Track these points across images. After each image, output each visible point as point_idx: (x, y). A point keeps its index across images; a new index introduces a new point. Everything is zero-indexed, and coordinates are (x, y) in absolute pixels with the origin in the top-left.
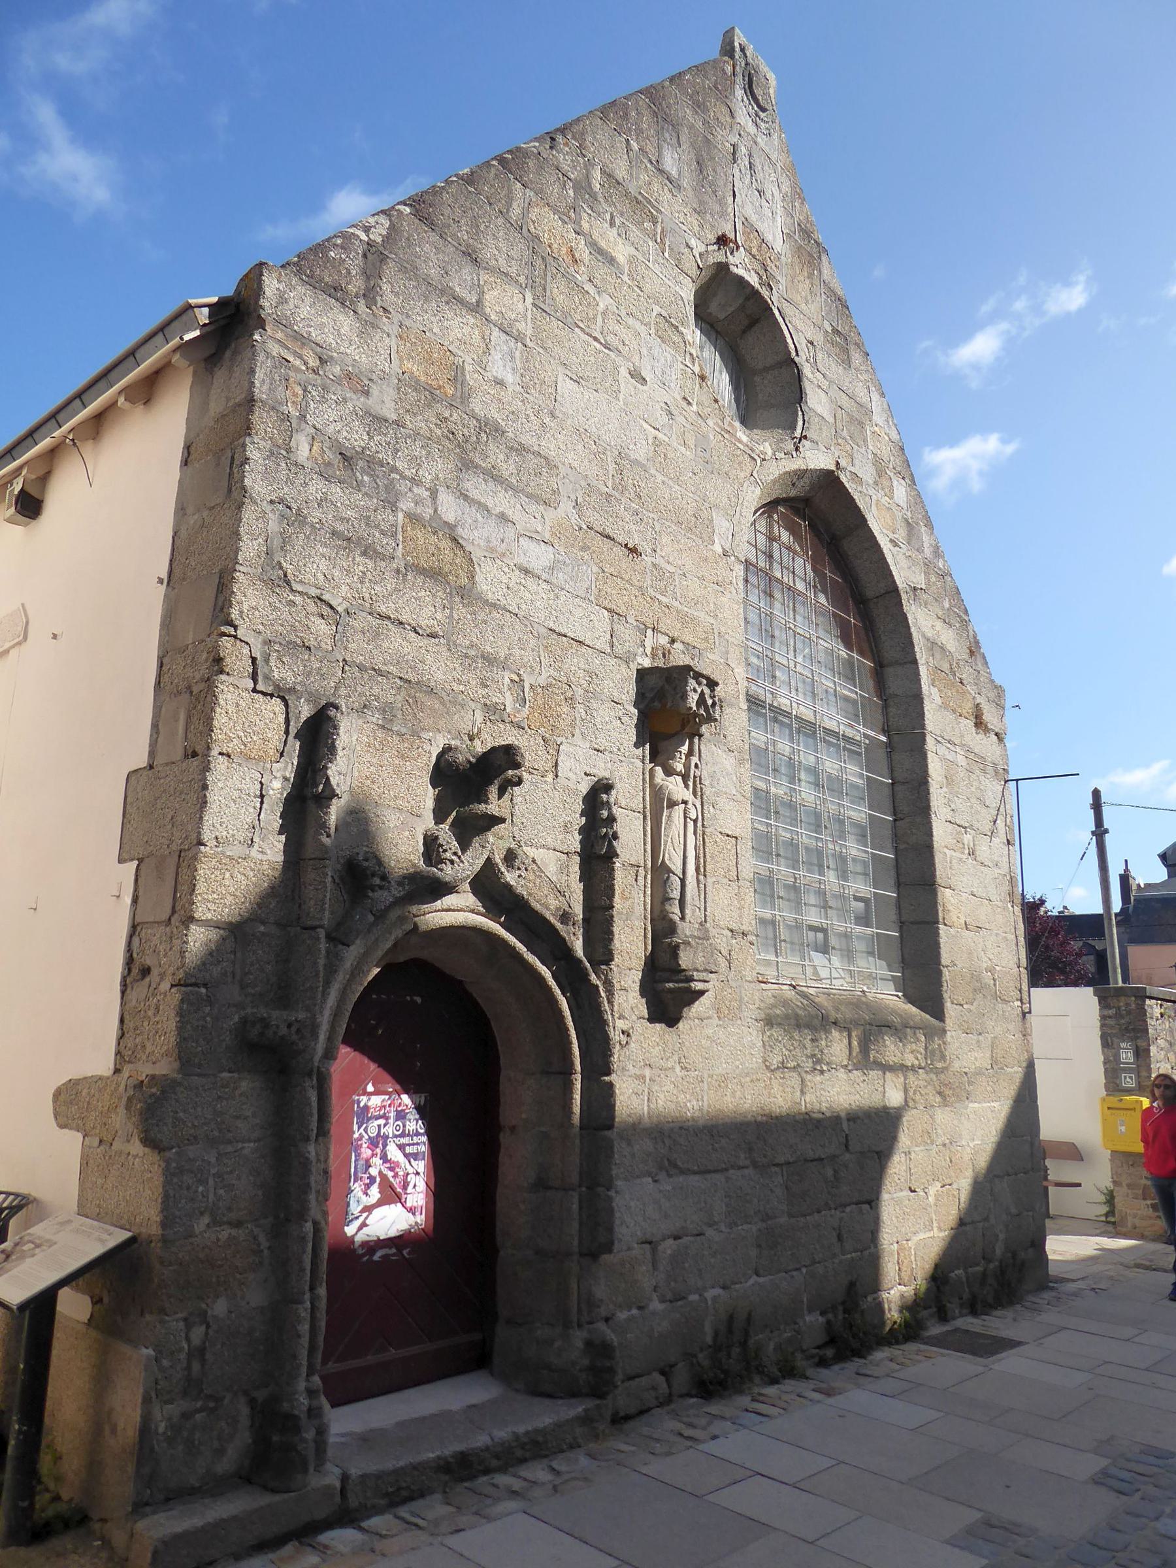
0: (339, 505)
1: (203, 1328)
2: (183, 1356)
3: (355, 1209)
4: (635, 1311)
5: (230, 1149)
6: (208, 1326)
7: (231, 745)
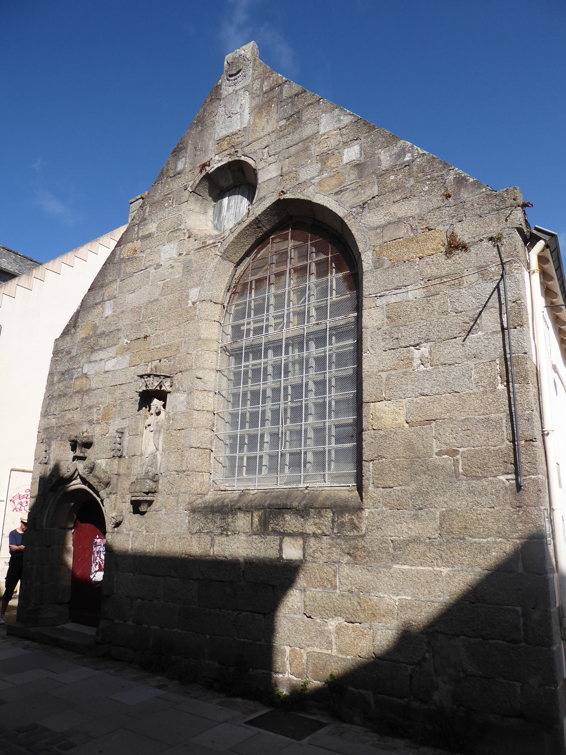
3: (93, 571)
4: (122, 622)
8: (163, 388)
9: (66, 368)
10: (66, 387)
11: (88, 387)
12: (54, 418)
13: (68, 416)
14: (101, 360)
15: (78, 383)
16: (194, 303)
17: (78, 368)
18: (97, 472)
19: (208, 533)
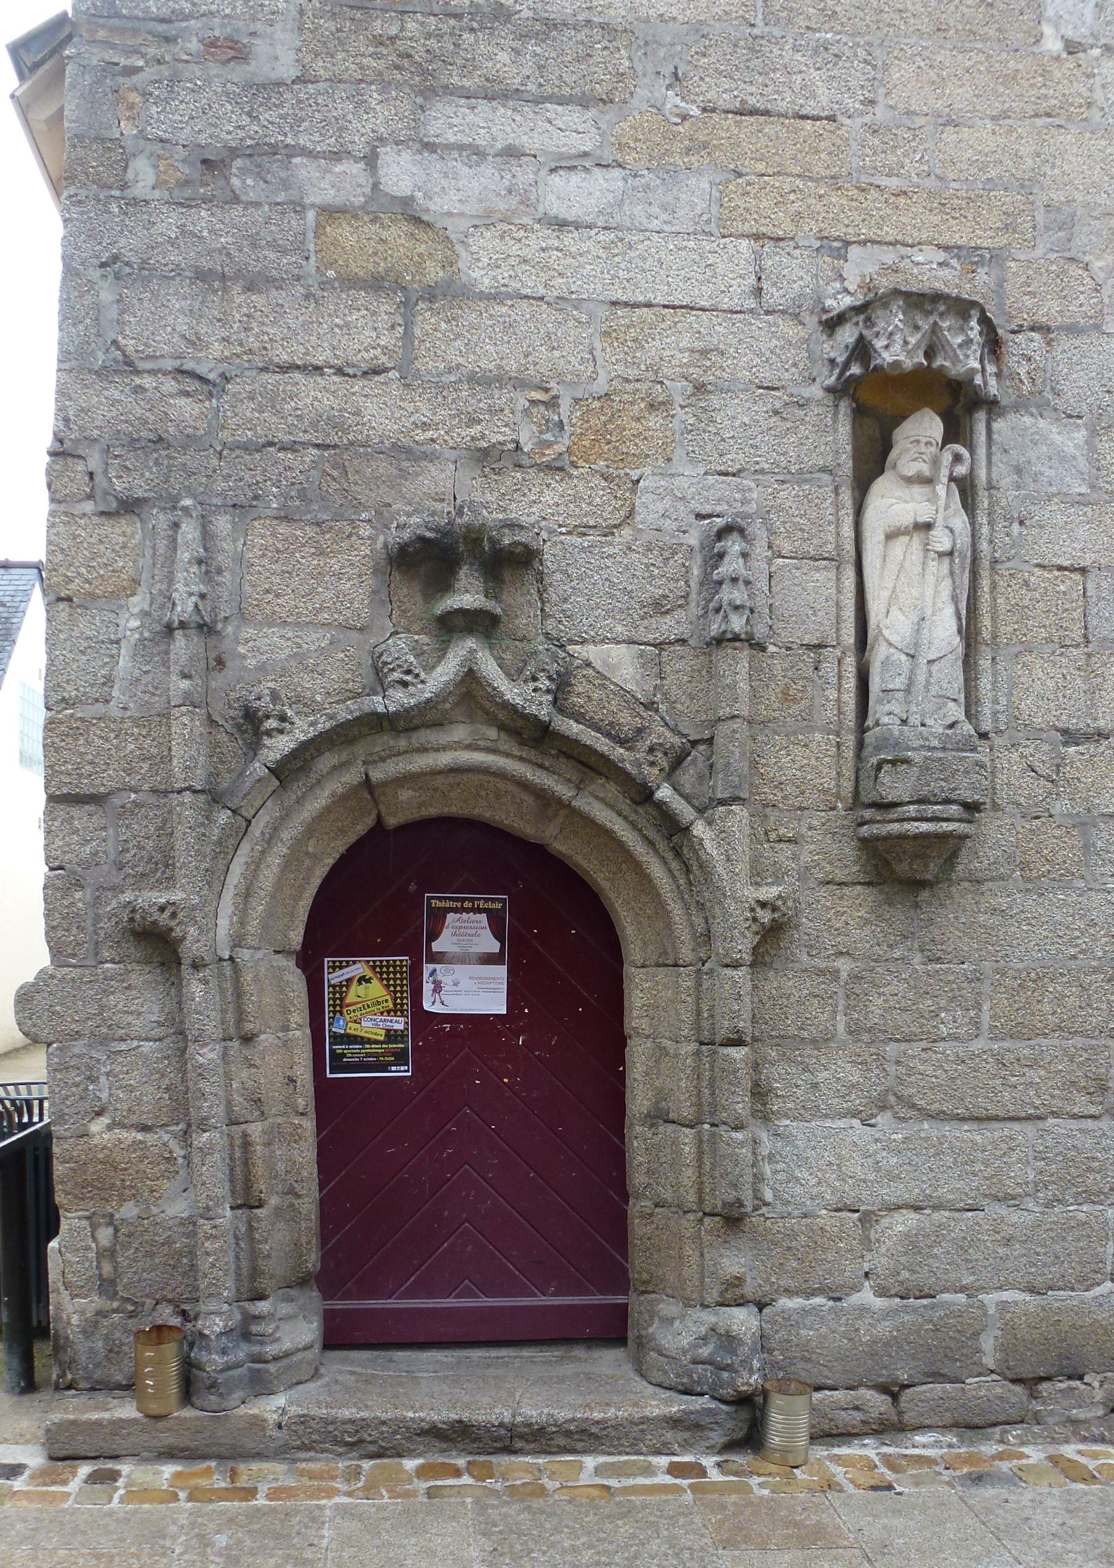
0: (205, 234)
1: (110, 1230)
2: (92, 1255)
5: (123, 1046)
6: (116, 1230)
7: (72, 586)
11: (434, 273)
12: (187, 394)
16: (1072, 47)
18: (581, 693)
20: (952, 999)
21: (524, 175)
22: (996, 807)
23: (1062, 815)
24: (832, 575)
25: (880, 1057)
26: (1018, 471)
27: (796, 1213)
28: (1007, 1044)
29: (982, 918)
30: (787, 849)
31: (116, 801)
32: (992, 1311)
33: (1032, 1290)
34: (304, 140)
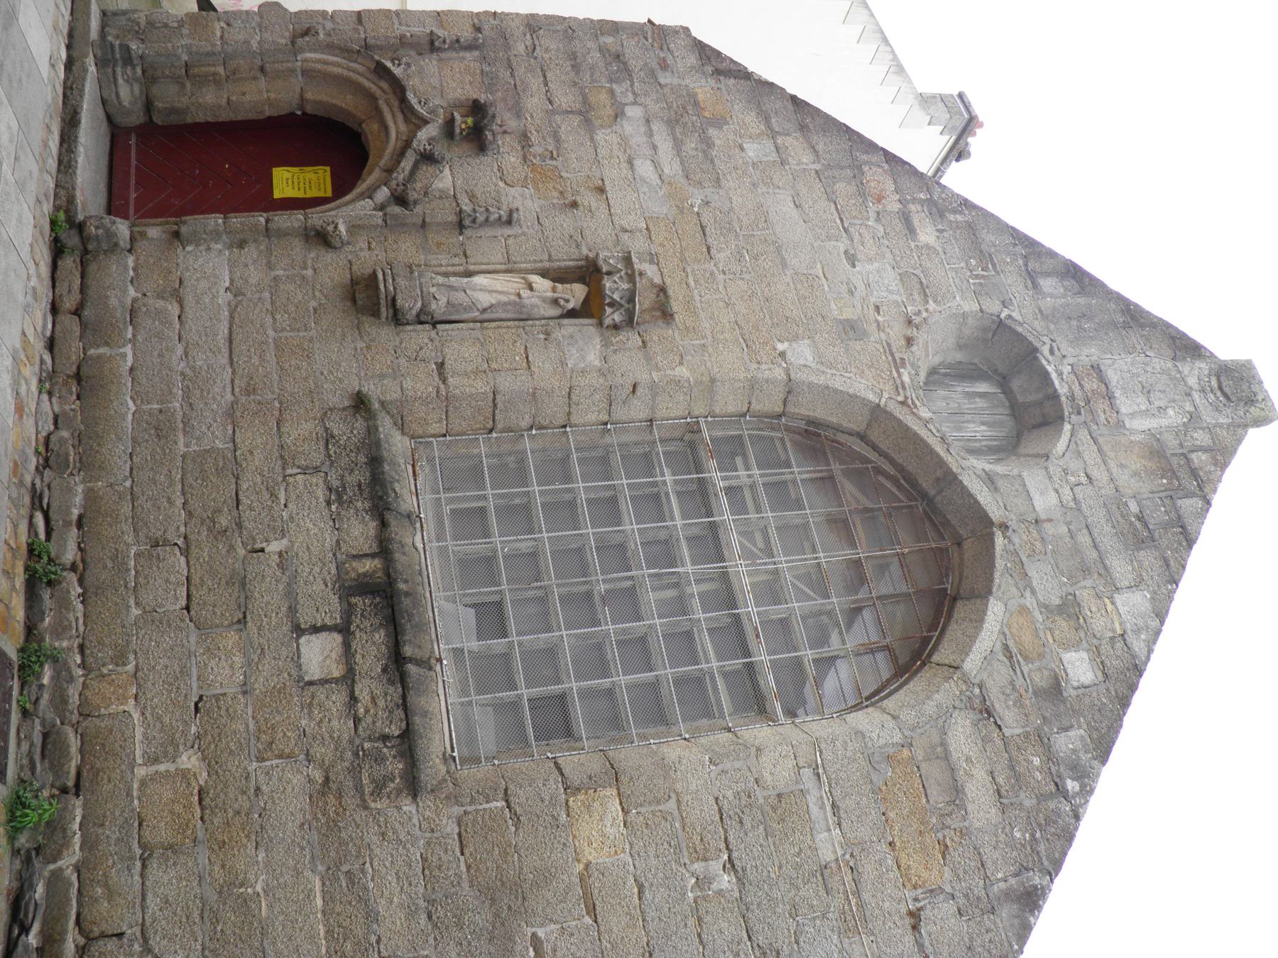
8: (608, 310)
9: (632, 62)
10: (592, 68)
11: (597, 123)
12: (527, 47)
13: (535, 83)
14: (655, 148)
15: (603, 97)
16: (782, 354)
17: (634, 93)
18: (426, 170)
19: (330, 456)
20: (294, 319)
21: (649, 152)
22: (398, 334)
23: (398, 364)
24: (501, 261)
25: (261, 292)
26: (571, 337)
27: (179, 261)
28: (272, 345)
29: (340, 330)
30: (365, 246)
31: (360, 28)
32: (121, 350)
33: (131, 369)
34: (636, 84)
